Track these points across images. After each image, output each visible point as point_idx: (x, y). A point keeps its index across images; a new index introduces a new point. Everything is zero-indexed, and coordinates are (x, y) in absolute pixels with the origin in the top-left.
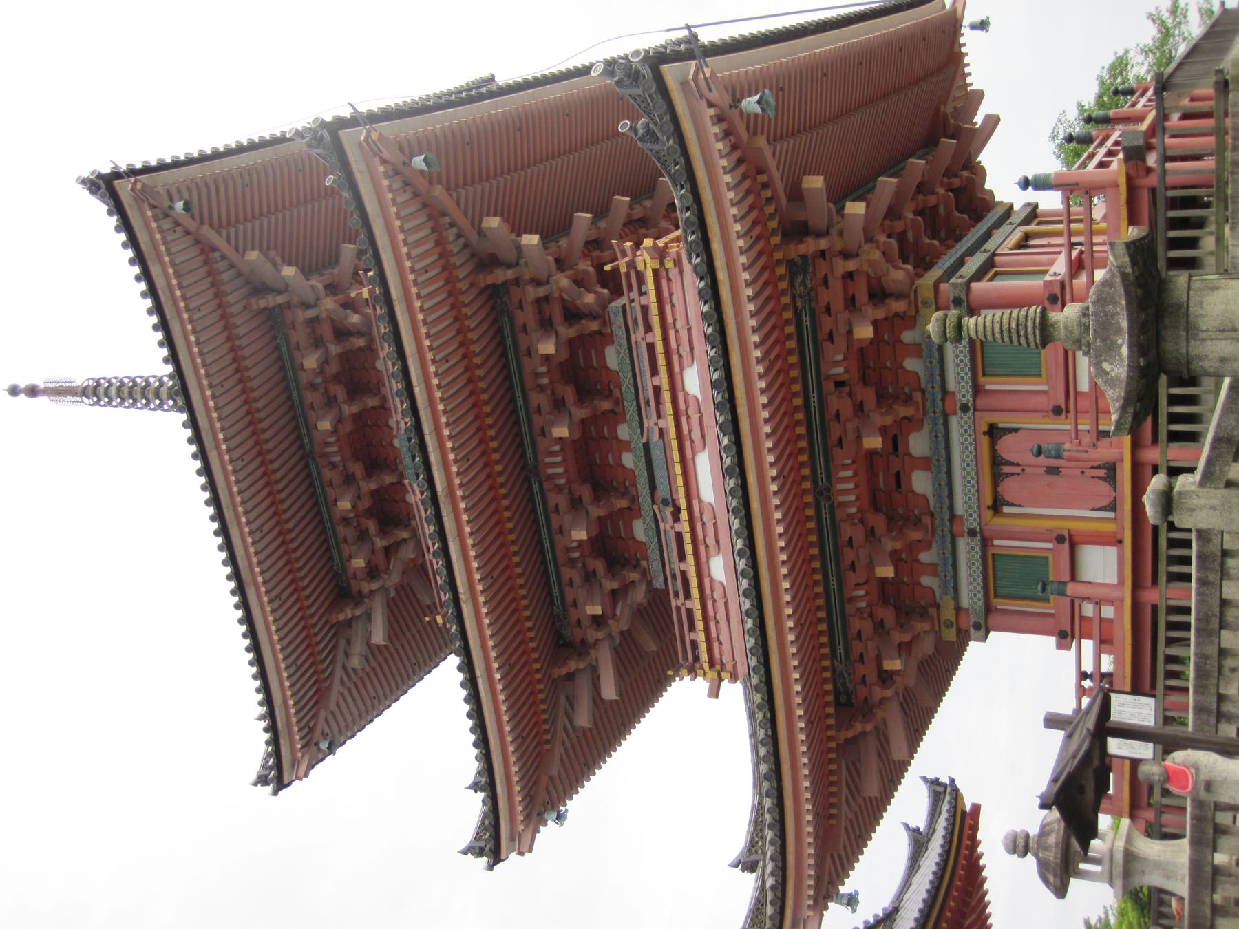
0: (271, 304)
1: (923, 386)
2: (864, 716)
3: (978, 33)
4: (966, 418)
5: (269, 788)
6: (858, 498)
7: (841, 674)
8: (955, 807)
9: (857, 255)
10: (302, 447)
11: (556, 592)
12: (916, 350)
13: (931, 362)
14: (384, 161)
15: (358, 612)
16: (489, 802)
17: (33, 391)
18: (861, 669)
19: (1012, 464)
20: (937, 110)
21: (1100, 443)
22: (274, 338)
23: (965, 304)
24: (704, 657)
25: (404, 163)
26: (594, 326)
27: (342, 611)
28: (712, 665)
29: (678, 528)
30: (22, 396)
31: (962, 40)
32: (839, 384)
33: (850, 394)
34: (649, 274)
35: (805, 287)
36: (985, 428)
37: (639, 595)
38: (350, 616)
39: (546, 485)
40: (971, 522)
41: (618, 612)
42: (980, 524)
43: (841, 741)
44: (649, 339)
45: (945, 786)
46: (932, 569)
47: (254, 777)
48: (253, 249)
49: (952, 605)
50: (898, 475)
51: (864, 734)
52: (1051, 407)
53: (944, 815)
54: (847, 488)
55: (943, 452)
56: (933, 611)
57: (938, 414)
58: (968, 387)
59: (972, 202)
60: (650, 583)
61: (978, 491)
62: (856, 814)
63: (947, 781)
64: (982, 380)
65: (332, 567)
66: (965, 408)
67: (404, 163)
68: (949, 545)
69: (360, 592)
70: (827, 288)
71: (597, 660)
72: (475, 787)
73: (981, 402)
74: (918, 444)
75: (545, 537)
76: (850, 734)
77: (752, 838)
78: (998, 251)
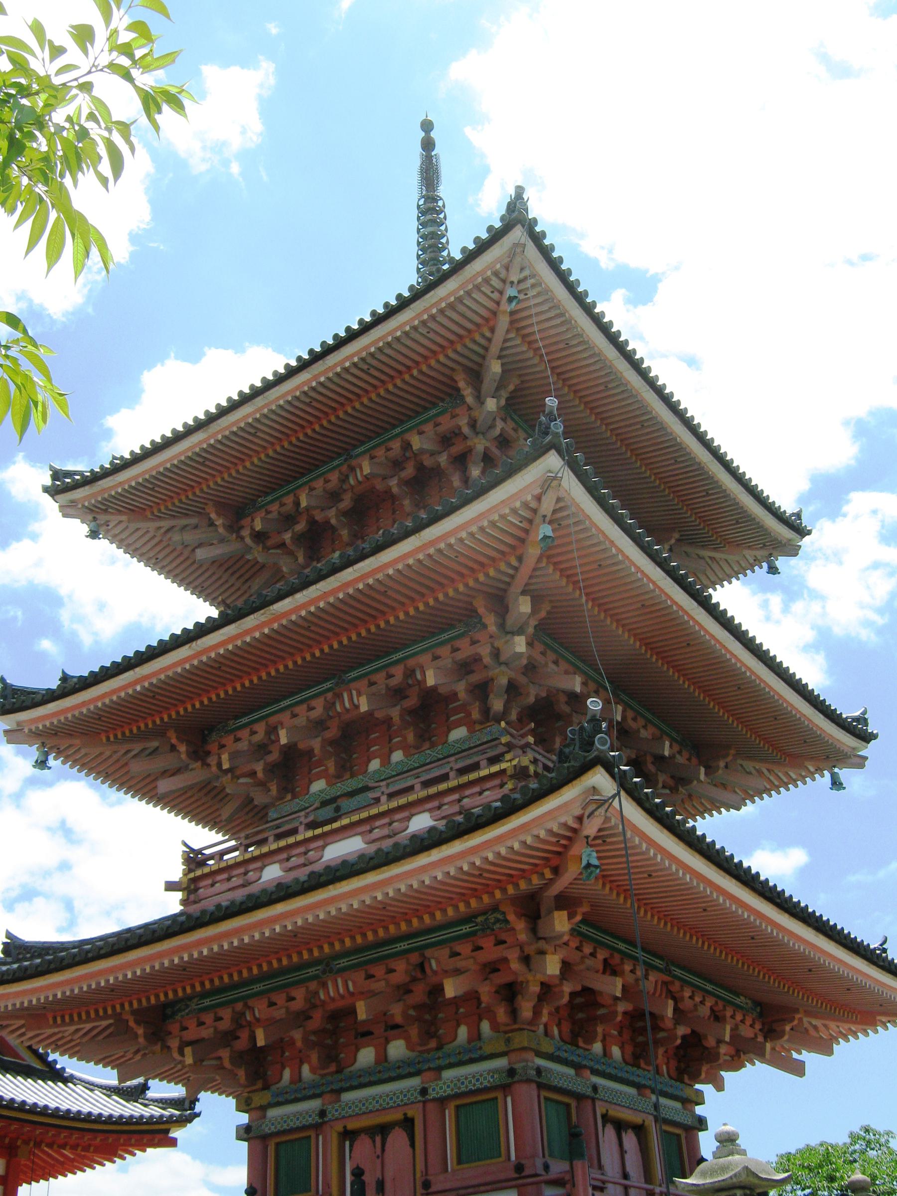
1: (446, 1047)
2: (153, 1034)
4: (416, 1094)
5: (48, 482)
6: (333, 999)
7: (187, 1006)
8: (176, 1121)
9: (530, 970)
10: (355, 447)
11: (245, 720)
13: (459, 1053)
15: (221, 530)
16: (39, 698)
17: (428, 145)
18: (192, 1024)
20: (796, 1011)
22: (443, 400)
23: (510, 1080)
24: (199, 872)
26: (476, 715)
27: (218, 514)
28: (195, 880)
29: (301, 828)
30: (423, 134)
32: (421, 967)
33: (414, 980)
34: (504, 766)
35: (494, 923)
36: (410, 1114)
38: (217, 523)
39: (329, 695)
41: (242, 780)
42: (330, 1120)
43: (125, 1017)
44: (452, 774)
45: (192, 1109)
48: (502, 365)
49: (264, 1102)
50: (371, 1033)
51: (136, 1036)
52: (430, 1178)
54: (336, 989)
55: (386, 1076)
56: (259, 1085)
57: (418, 1066)
58: (441, 1093)
60: (272, 805)
61: (357, 1115)
62: (71, 1040)
63: (197, 1110)
64: (452, 1105)
65: (260, 497)
66: (424, 1091)
67: (545, 516)
68: (311, 1093)
69: (242, 527)
70: (495, 945)
71: (192, 770)
72: (65, 678)
73: (430, 1106)
74: (397, 1049)
75: (287, 702)
76: (132, 1023)
77: (32, 947)
78: (598, 1103)
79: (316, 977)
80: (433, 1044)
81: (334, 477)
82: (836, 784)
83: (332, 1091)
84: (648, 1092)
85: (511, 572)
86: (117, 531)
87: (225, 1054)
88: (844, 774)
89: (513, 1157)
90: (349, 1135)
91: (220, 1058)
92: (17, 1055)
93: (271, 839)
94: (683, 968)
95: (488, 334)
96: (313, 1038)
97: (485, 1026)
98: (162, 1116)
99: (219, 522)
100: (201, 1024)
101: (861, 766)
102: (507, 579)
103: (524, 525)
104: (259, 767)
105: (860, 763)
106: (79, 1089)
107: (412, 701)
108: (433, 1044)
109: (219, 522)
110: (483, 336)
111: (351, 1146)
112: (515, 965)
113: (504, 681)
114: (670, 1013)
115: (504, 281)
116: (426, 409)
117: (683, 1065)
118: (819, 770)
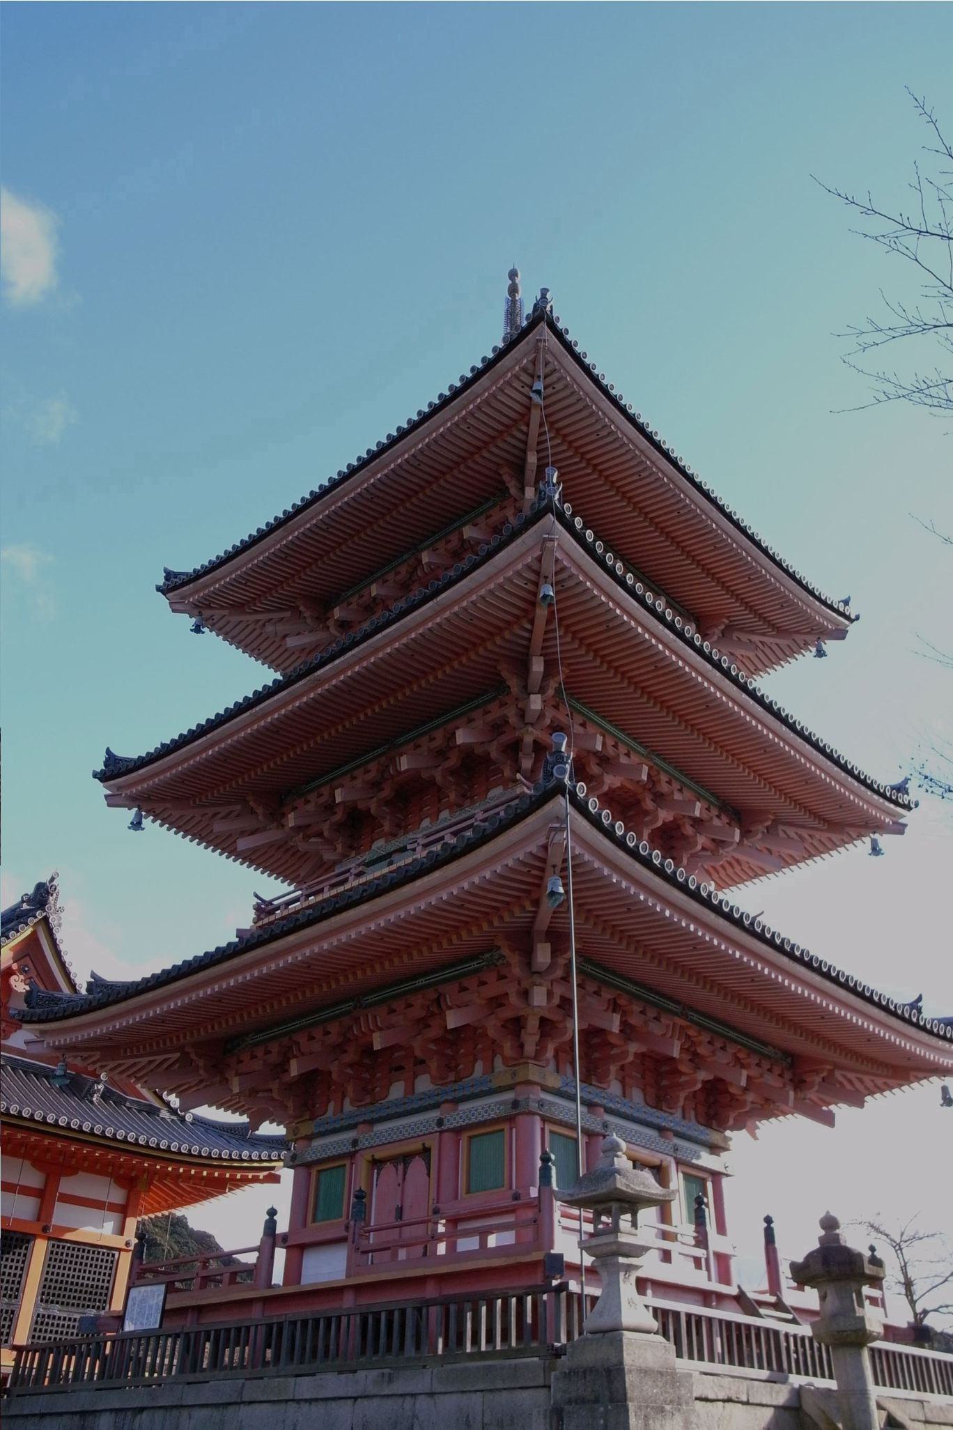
0: (509, 485)
4: (433, 1125)
5: (161, 582)
10: (422, 542)
15: (309, 621)
16: (131, 765)
19: (405, 1174)
25: (546, 577)
37: (328, 856)
41: (312, 840)
47: (171, 568)
52: (440, 1205)
58: (455, 1124)
59: (718, 1109)
74: (424, 1084)
75: (347, 768)
76: (193, 1056)
79: (348, 1012)
80: (452, 1077)
81: (403, 569)
82: (876, 850)
83: (364, 1122)
84: (670, 1134)
85: (526, 635)
86: (221, 624)
87: (274, 1085)
88: (884, 840)
90: (377, 1163)
91: (271, 1090)
93: (326, 889)
94: (697, 1012)
95: (524, 428)
97: (498, 1061)
99: (307, 614)
100: (253, 1057)
101: (902, 832)
102: (525, 643)
103: (530, 587)
104: (325, 827)
107: (453, 761)
108: (452, 1077)
109: (307, 614)
110: (521, 431)
113: (528, 739)
115: (532, 377)
116: (481, 504)
117: (712, 1112)
118: (859, 836)
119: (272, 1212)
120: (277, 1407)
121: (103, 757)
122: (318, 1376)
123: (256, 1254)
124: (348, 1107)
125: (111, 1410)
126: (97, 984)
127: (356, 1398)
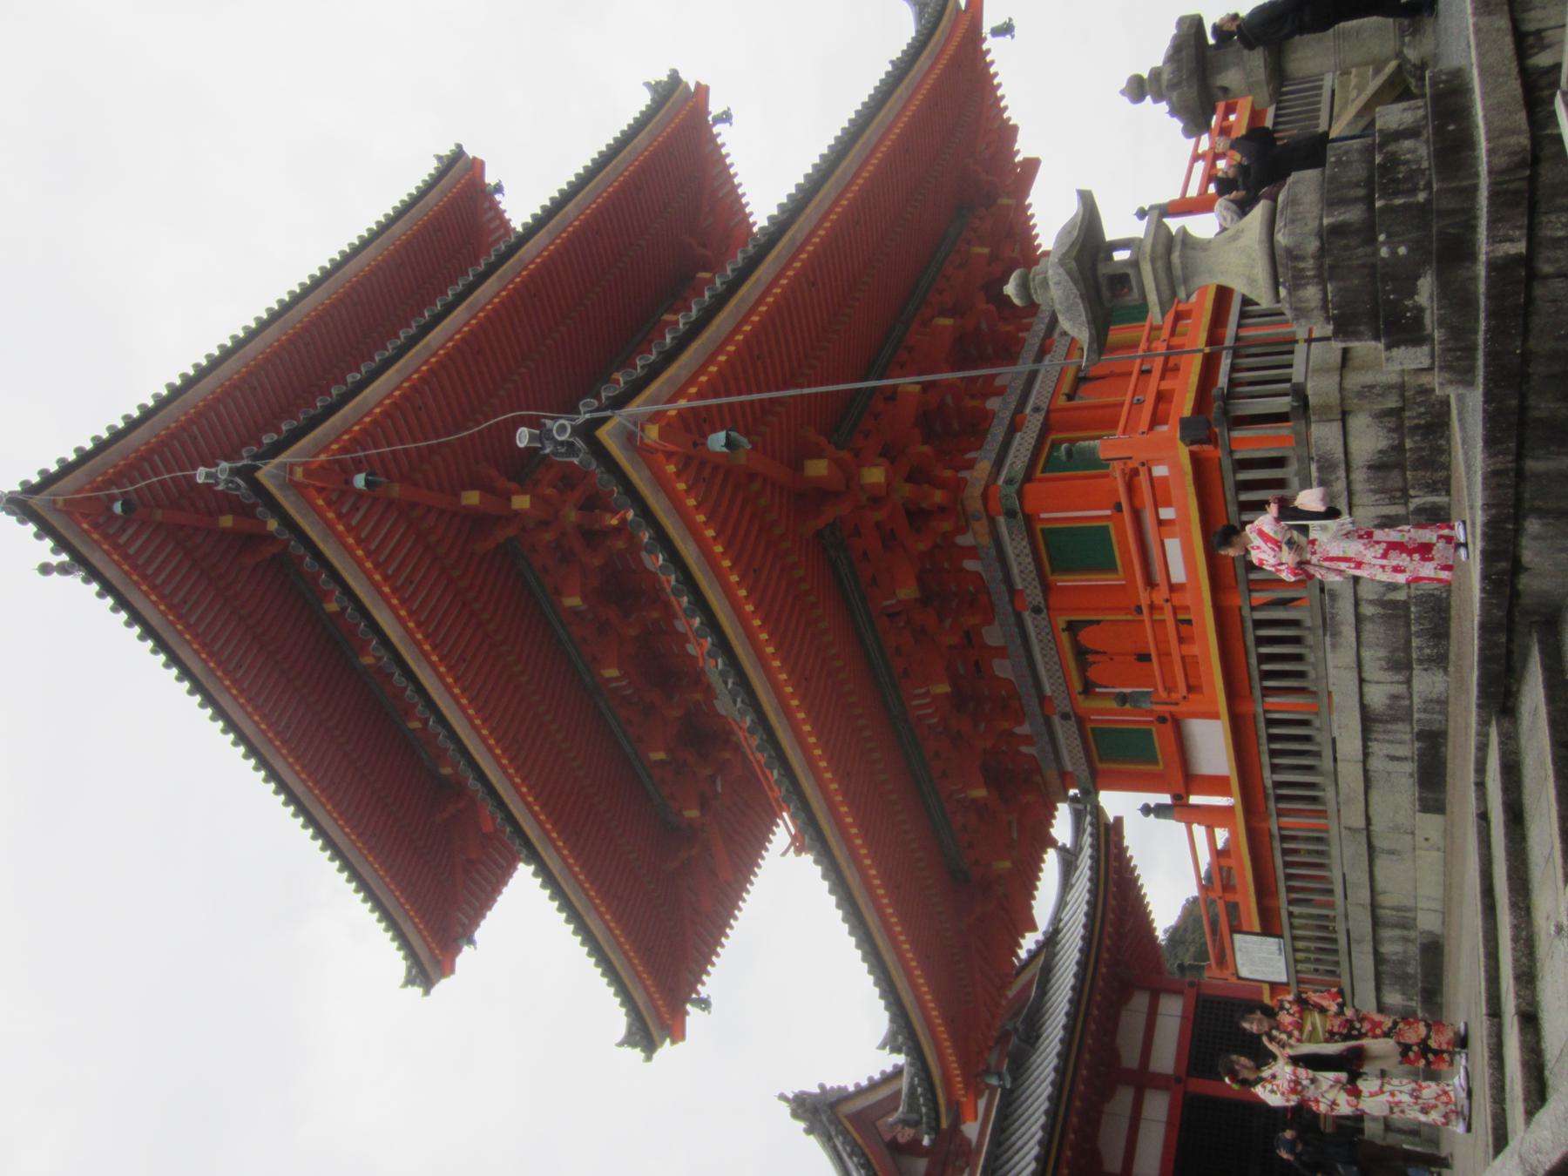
3: (1000, 39)
4: (1039, 618)
12: (972, 552)
14: (320, 490)
19: (1097, 653)
21: (1191, 697)
26: (621, 544)
31: (985, 47)
40: (1062, 704)
41: (719, 789)
46: (1028, 740)
50: (977, 663)
53: (1089, 829)
56: (1038, 778)
58: (1038, 591)
64: (1052, 578)
74: (993, 636)
89: (1108, 512)
92: (1030, 984)
96: (982, 727)
98: (1091, 835)
105: (702, 92)
106: (1065, 916)
111: (1100, 686)
112: (879, 516)
114: (948, 322)
119: (1146, 810)
120: (1374, 783)
121: (627, 1050)
122: (1336, 734)
123: (1195, 827)
124: (1024, 729)
125: (1378, 989)
126: (891, 1043)
127: (1361, 681)
